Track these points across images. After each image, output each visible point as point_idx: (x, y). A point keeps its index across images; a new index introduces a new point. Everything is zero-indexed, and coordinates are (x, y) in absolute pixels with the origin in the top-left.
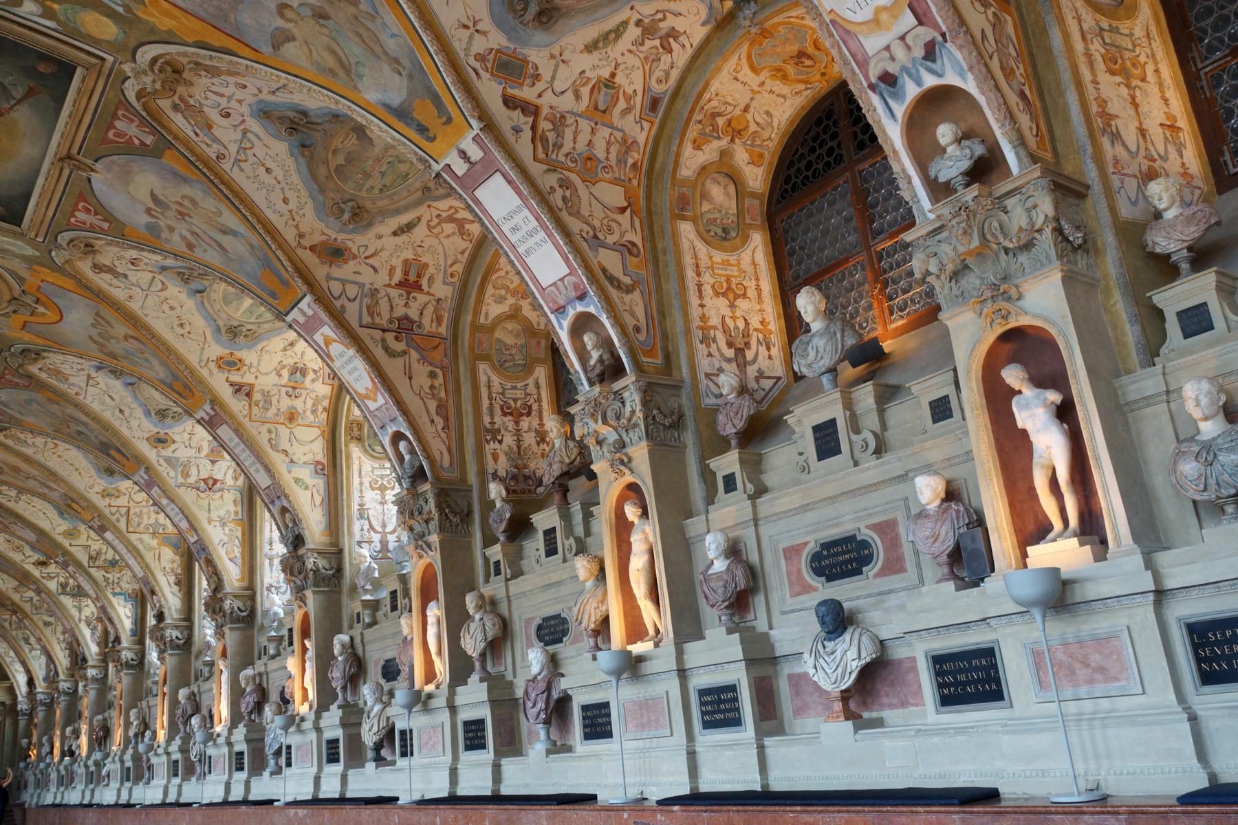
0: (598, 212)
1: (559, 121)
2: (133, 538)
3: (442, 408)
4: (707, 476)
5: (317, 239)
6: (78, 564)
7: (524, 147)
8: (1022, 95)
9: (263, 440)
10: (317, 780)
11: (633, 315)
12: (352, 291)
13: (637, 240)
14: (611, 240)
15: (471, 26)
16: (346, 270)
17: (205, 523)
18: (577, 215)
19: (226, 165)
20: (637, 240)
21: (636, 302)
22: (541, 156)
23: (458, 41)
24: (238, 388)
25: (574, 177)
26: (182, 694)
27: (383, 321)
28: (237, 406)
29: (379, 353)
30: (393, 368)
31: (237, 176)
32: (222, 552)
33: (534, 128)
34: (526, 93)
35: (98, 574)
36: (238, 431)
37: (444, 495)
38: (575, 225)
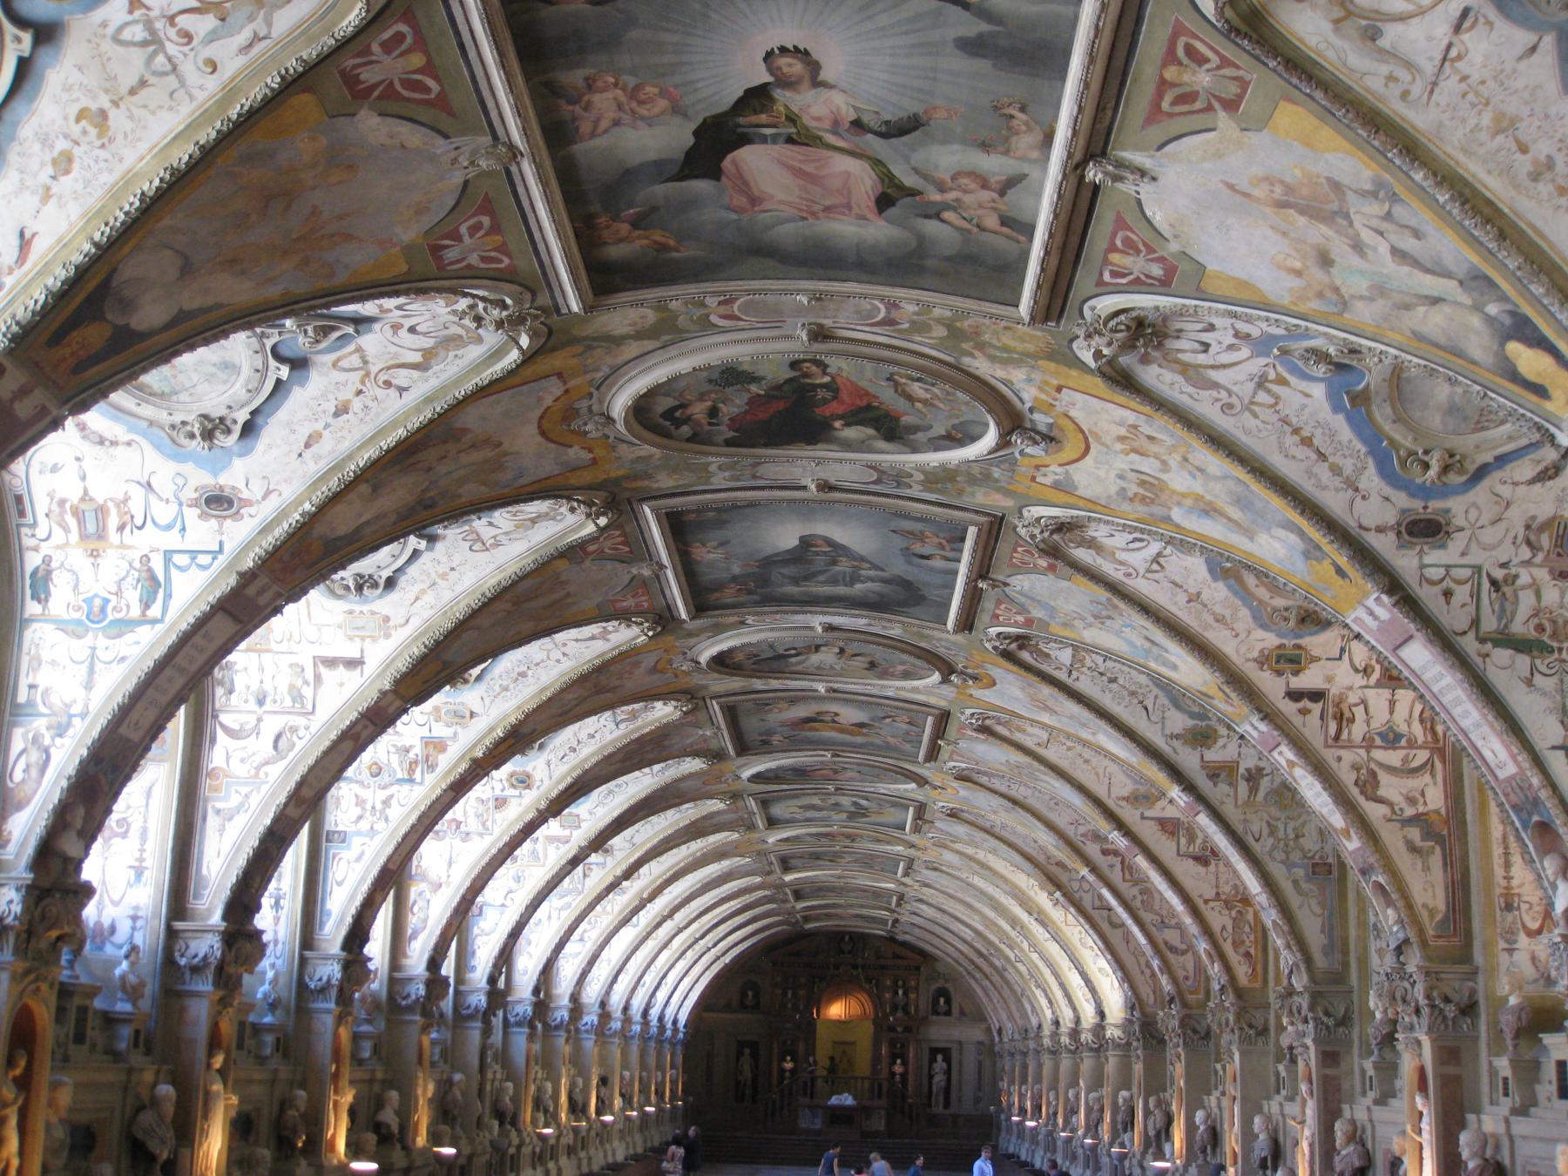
4: (1216, 1072)
6: (1007, 959)
7: (1116, 876)
8: (1247, 955)
11: (1185, 969)
14: (1173, 922)
17: (1066, 969)
18: (1151, 910)
19: (997, 830)
21: (1188, 961)
22: (1128, 876)
23: (1070, 832)
29: (1105, 926)
30: (1115, 936)
32: (1080, 994)
33: (1122, 862)
38: (1147, 917)
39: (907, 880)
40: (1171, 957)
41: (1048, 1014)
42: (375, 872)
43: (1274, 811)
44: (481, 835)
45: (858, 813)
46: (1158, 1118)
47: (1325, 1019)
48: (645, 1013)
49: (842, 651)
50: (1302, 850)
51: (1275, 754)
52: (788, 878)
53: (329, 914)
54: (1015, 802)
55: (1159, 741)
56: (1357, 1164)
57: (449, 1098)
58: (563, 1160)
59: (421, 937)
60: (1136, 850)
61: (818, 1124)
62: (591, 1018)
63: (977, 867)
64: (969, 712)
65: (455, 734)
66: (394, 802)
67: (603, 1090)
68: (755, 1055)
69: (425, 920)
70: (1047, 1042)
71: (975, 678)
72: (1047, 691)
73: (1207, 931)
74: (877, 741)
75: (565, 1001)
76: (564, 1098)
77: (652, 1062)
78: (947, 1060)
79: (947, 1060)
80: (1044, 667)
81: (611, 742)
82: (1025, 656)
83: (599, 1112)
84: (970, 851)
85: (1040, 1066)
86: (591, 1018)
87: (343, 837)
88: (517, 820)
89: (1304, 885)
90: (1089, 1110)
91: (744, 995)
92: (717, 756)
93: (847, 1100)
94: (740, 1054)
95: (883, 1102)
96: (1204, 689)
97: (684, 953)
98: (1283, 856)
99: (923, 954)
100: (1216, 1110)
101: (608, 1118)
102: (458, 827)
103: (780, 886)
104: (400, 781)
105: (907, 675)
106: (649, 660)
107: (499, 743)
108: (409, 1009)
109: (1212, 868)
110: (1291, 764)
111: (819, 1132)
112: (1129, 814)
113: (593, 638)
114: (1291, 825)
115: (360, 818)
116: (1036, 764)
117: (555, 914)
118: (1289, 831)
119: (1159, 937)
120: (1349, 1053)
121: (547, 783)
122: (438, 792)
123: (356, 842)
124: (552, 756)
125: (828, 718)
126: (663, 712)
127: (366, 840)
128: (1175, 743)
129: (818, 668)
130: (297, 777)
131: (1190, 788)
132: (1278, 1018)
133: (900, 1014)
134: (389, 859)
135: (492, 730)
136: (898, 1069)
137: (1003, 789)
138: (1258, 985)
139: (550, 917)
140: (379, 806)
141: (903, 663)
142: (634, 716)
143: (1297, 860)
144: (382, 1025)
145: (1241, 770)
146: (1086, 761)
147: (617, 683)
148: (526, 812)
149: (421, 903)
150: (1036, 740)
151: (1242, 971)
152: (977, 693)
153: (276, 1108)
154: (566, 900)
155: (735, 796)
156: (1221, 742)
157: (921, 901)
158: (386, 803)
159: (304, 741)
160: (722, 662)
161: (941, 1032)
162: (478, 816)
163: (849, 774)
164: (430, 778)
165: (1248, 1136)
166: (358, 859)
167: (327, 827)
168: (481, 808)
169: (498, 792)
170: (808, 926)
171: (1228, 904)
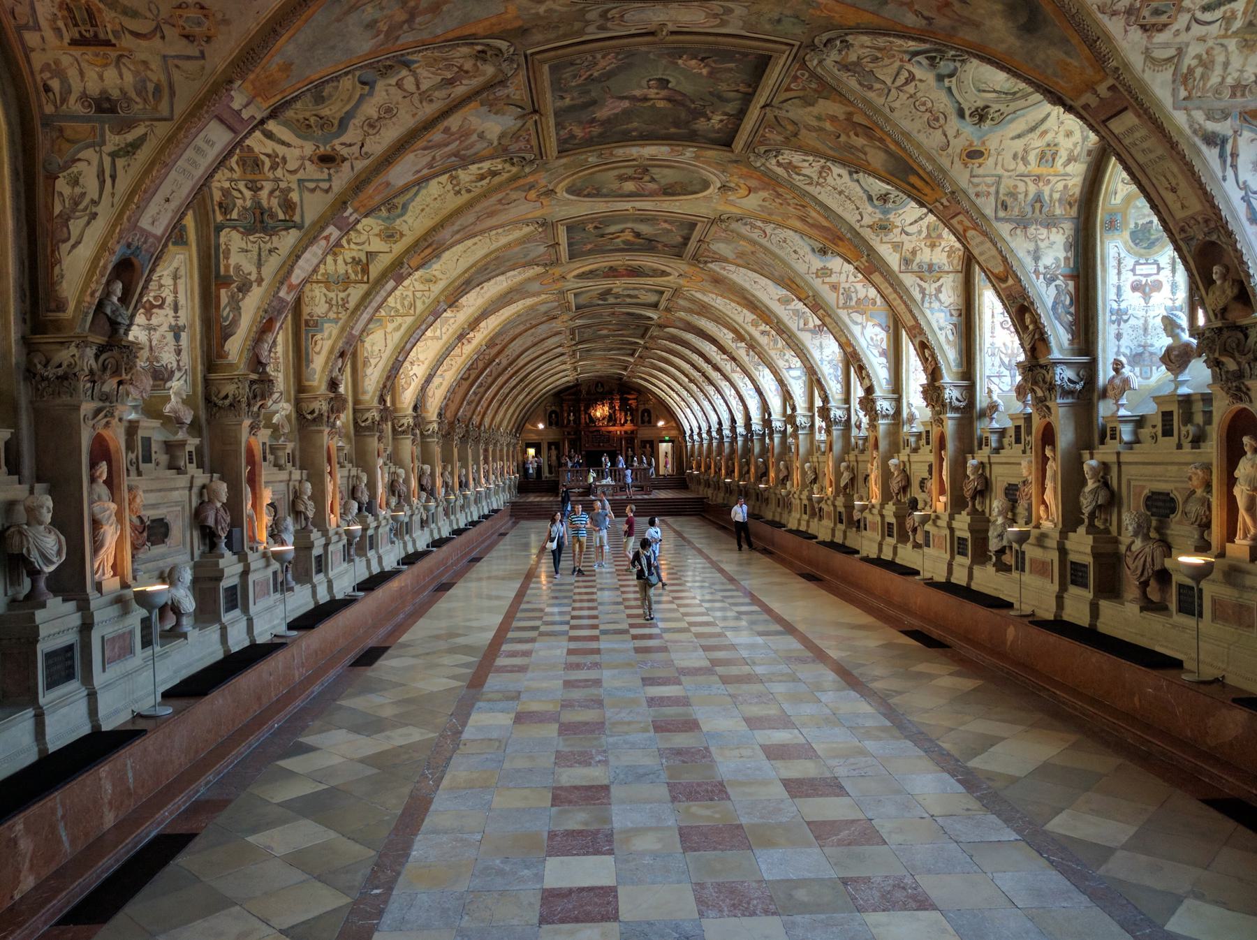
24: (763, 333)
90: (778, 471)
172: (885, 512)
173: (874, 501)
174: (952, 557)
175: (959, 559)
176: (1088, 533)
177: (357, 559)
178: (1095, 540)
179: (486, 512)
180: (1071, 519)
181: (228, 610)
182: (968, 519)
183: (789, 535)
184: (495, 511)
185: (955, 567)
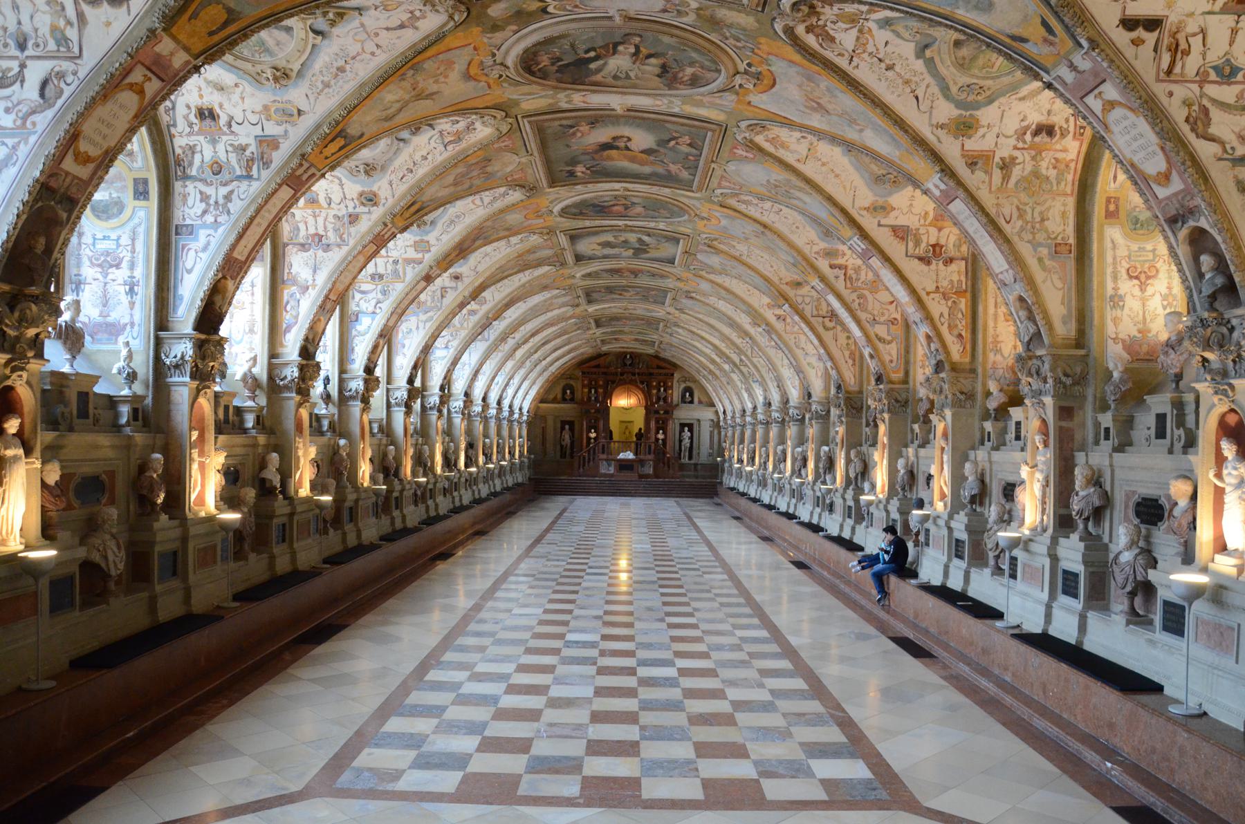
0: (877, 305)
1: (857, 270)
2: (755, 360)
3: (852, 355)
5: (788, 280)
6: (735, 364)
7: (840, 285)
9: (792, 343)
10: (812, 513)
11: (890, 355)
12: (807, 300)
13: (898, 317)
14: (882, 319)
15: (811, 243)
16: (805, 290)
18: (866, 310)
19: (744, 258)
20: (898, 317)
22: (849, 285)
24: (779, 317)
25: (866, 293)
26: (780, 448)
27: (823, 313)
28: (779, 326)
29: (821, 330)
30: (828, 336)
31: (748, 260)
34: (840, 261)
35: (744, 369)
36: (780, 337)
37: (848, 400)
38: (863, 316)
39: (672, 310)
40: (880, 346)
41: (761, 399)
42: (219, 259)
43: (1023, 196)
44: (339, 246)
45: (641, 250)
46: (856, 467)
47: (1064, 379)
48: (499, 403)
49: (637, 47)
50: (1046, 231)
51: (1090, 100)
52: (591, 309)
53: (182, 299)
54: (765, 226)
55: (926, 132)
56: (1097, 503)
57: (336, 458)
58: (440, 499)
59: (294, 330)
60: (874, 252)
61: (612, 470)
62: (457, 403)
63: (723, 292)
64: (743, 124)
65: (286, 132)
66: (234, 196)
67: (470, 451)
68: (572, 430)
69: (296, 317)
70: (760, 417)
71: (758, 76)
72: (826, 82)
73: (928, 318)
74: (660, 170)
75: (437, 390)
76: (439, 459)
77: (505, 433)
78: (691, 430)
79: (691, 430)
80: (829, 54)
81: (441, 163)
82: (811, 40)
83: (467, 466)
84: (719, 279)
85: (754, 432)
86: (457, 403)
87: (191, 230)
88: (368, 233)
89: (1047, 262)
90: (794, 460)
91: (564, 393)
92: (531, 189)
93: (629, 455)
94: (563, 429)
95: (651, 457)
96: (1016, 31)
97: (523, 363)
98: (1030, 237)
99: (675, 366)
100: (912, 458)
101: (473, 469)
102: (320, 240)
103: (584, 318)
104: (239, 178)
105: (695, 82)
106: (461, 59)
107: (328, 140)
108: (287, 388)
109: (933, 266)
110: (1110, 105)
111: (612, 475)
112: (868, 222)
113: (402, 26)
114: (1038, 209)
115: (205, 212)
116: (793, 179)
117: (421, 325)
118: (1036, 215)
119: (871, 331)
120: (1082, 407)
121: (391, 201)
122: (273, 185)
123: (202, 234)
124: (393, 176)
125: (622, 145)
126: (483, 131)
127: (211, 232)
128: (940, 132)
129: (615, 77)
130: (66, 126)
131: (947, 171)
132: (984, 384)
133: (661, 403)
134: (233, 247)
135: (318, 126)
136: (661, 436)
137: (757, 215)
138: (967, 360)
139: (418, 328)
140: (221, 201)
141: (692, 64)
142: (458, 138)
143: (1041, 240)
144: (263, 401)
145: (997, 159)
146: (837, 176)
147: (435, 88)
148: (375, 225)
149: (292, 303)
150: (797, 157)
151: (955, 350)
152: (756, 99)
153: (134, 470)
154: (431, 314)
155: (551, 231)
156: (981, 131)
157: (678, 326)
158: (228, 198)
159: (73, 87)
160: (529, 64)
161: (685, 414)
162: (336, 230)
163: (639, 209)
164: (266, 174)
165: (958, 479)
166: (205, 249)
167: (176, 222)
168: (338, 223)
169: (351, 210)
170: (605, 348)
171: (945, 296)
172: (890, 508)
173: (881, 496)
174: (950, 559)
175: (956, 561)
176: (1081, 539)
177: (331, 531)
178: (1086, 548)
179: (498, 489)
180: (1064, 523)
181: (161, 580)
182: (965, 520)
183: (798, 527)
184: (508, 489)
185: (952, 570)
